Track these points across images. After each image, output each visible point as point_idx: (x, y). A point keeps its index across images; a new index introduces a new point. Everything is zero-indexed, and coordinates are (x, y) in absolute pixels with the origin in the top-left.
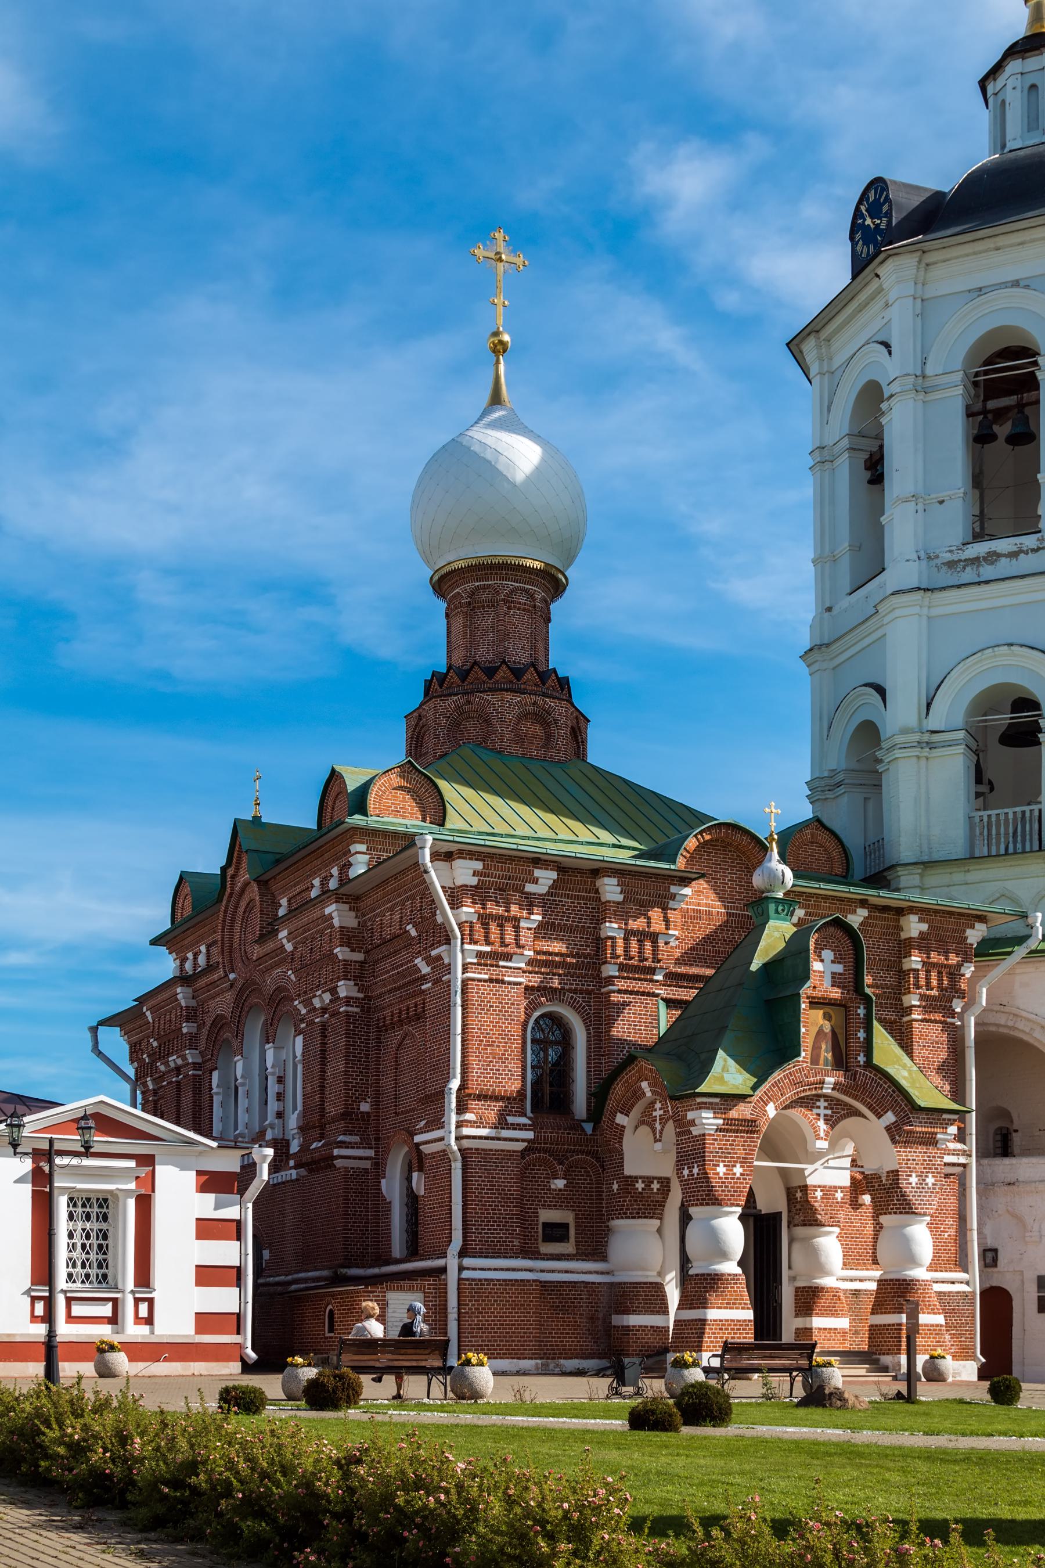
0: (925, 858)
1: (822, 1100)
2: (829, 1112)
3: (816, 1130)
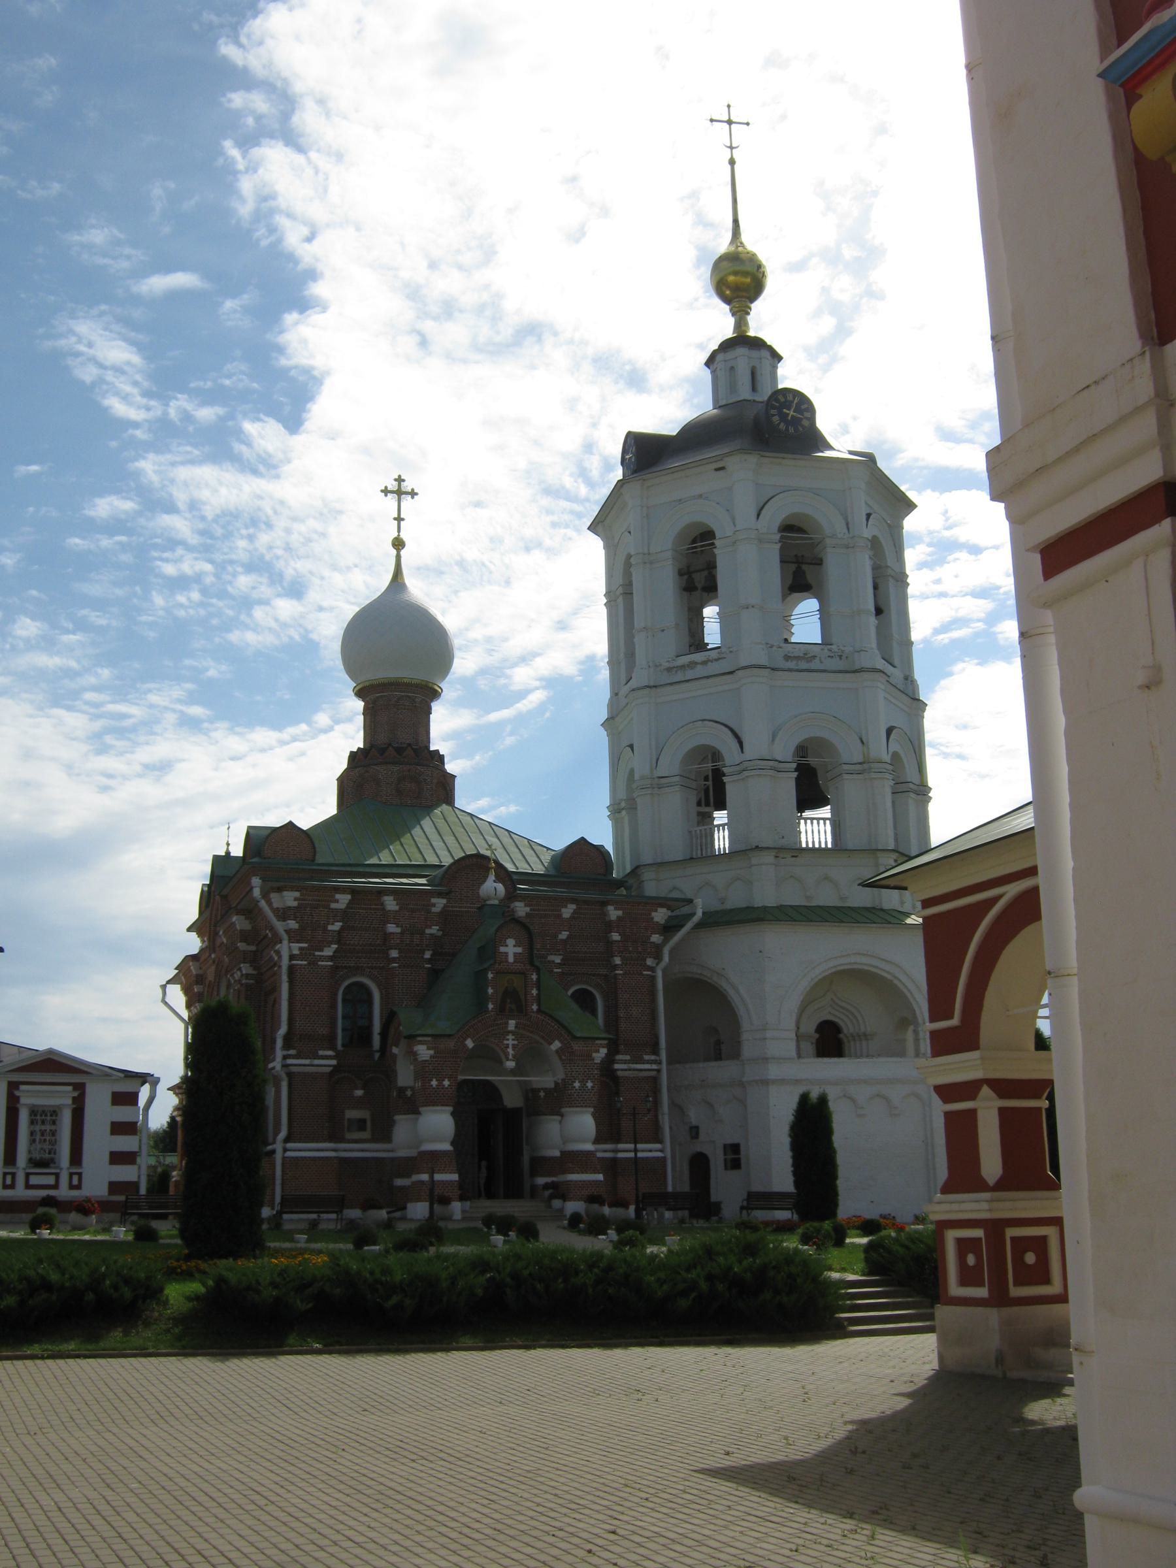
0: (659, 861)
3: (506, 1055)
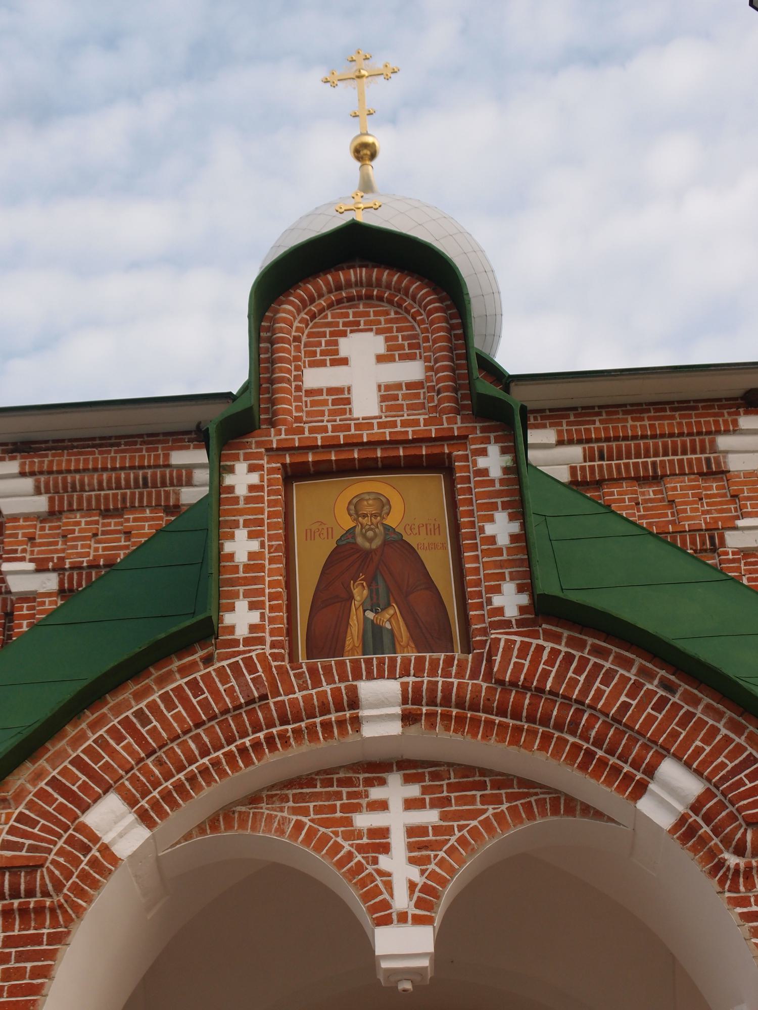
1: (394, 779)
2: (430, 817)
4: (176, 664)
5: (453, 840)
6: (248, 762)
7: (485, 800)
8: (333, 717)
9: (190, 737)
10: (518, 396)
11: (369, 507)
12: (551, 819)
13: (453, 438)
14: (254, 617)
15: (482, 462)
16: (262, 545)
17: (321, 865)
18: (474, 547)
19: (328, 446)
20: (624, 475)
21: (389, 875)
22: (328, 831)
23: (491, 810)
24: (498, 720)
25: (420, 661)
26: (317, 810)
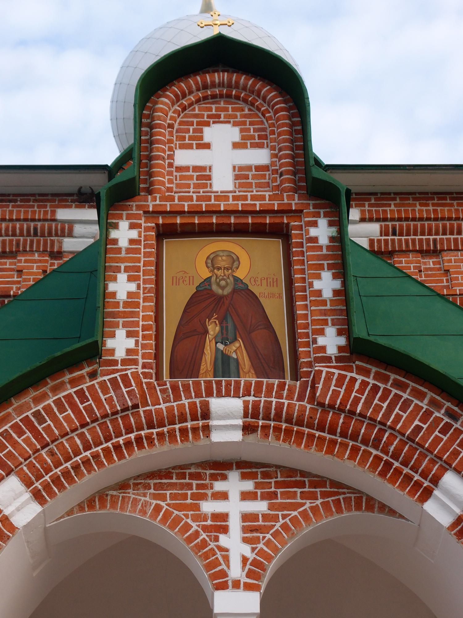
1: (234, 475)
2: (260, 507)
4: (67, 377)
5: (278, 526)
6: (121, 456)
7: (304, 496)
8: (189, 424)
9: (77, 435)
10: (342, 181)
11: (222, 262)
12: (354, 513)
13: (291, 211)
14: (131, 343)
15: (313, 232)
16: (139, 287)
17: (174, 541)
18: (305, 298)
19: (192, 213)
20: (411, 248)
21: (227, 550)
22: (181, 514)
23: (308, 504)
24: (317, 434)
25: (259, 385)
26: (173, 497)
